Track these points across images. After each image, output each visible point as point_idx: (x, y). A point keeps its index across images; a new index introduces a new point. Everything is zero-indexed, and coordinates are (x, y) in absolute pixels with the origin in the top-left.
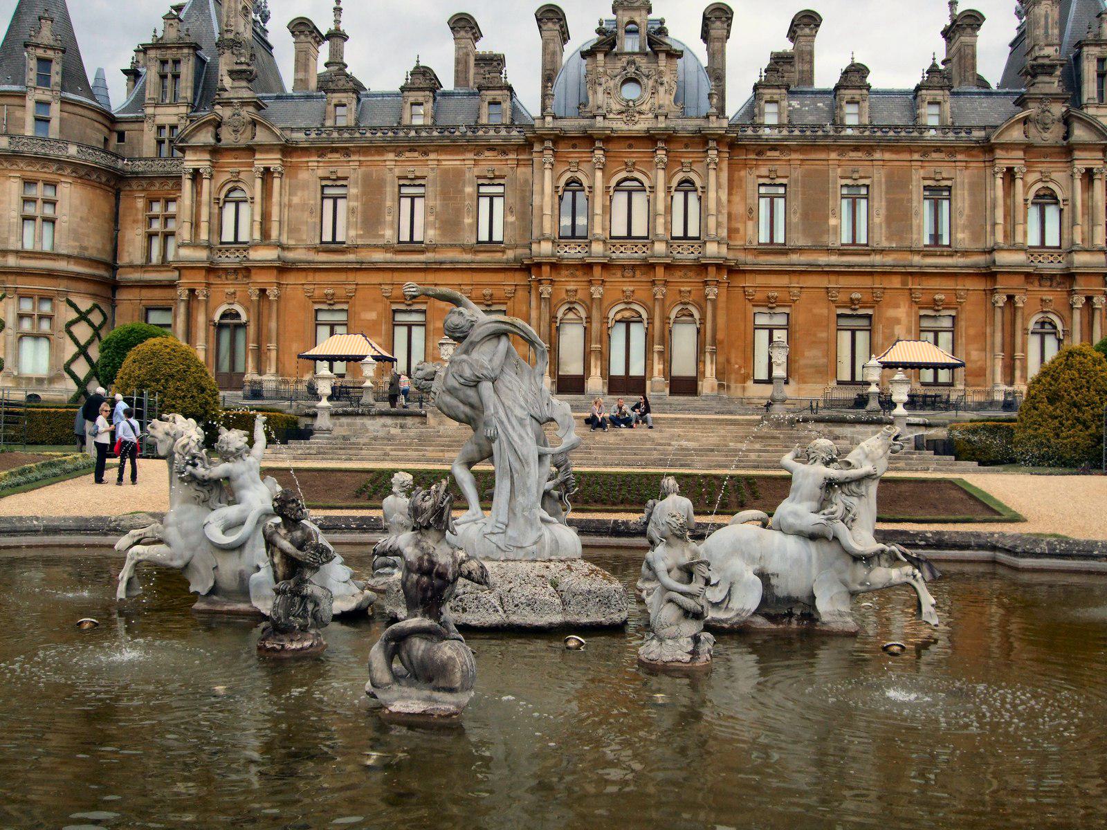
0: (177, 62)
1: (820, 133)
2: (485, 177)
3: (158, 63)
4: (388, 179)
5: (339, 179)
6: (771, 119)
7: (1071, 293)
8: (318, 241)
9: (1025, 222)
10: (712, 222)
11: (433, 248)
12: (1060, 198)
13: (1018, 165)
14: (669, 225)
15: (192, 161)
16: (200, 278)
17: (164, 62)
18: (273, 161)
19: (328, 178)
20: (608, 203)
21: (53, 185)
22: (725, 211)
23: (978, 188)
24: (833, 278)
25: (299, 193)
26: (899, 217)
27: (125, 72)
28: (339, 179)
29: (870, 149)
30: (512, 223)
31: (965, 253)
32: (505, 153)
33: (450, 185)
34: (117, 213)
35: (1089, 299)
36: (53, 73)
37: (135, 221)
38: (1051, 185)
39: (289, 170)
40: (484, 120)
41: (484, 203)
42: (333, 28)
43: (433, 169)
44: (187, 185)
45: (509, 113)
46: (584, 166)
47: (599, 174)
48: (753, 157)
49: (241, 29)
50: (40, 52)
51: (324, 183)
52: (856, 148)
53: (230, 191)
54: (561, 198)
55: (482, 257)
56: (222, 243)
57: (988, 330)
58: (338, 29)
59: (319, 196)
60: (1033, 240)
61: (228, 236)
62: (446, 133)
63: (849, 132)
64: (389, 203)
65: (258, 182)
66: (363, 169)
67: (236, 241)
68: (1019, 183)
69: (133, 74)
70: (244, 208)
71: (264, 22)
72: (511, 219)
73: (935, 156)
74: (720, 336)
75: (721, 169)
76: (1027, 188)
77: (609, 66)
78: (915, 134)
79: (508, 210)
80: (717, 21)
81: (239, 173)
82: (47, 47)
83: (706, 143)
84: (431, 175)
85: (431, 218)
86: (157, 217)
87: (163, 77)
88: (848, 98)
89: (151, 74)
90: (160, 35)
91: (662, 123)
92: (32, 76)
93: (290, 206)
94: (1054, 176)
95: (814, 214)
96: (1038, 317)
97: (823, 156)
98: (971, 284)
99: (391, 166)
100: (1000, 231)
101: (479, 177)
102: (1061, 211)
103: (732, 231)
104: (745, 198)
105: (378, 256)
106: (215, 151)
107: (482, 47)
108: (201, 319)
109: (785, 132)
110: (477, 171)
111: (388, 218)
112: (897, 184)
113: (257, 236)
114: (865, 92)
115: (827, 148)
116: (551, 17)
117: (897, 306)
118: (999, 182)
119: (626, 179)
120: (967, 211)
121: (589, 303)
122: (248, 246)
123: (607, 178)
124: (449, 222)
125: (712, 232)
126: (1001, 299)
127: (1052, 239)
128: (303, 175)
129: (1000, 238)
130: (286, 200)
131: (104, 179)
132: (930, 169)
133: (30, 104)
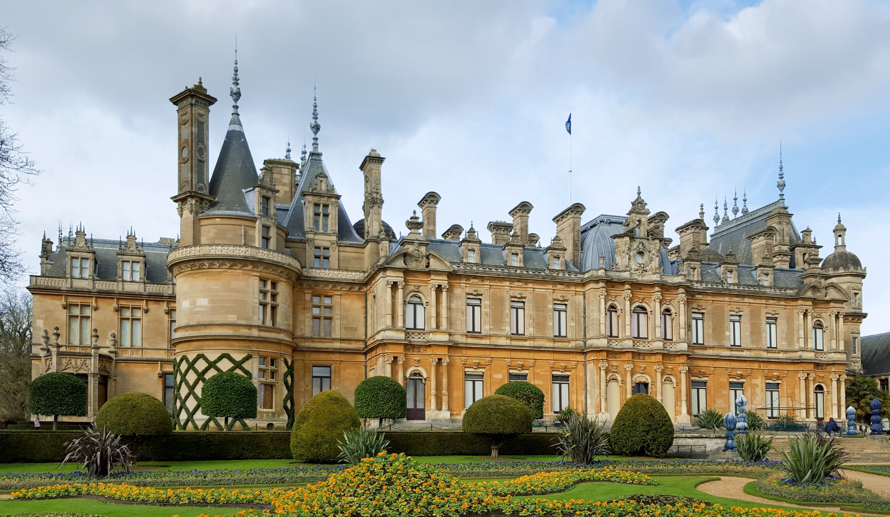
0: (326, 206)
5: (478, 295)
11: (533, 338)
16: (445, 351)
17: (317, 205)
18: (443, 281)
19: (472, 294)
23: (790, 320)
24: (729, 363)
26: (756, 332)
28: (478, 295)
29: (744, 296)
52: (737, 296)
55: (557, 345)
65: (434, 293)
85: (531, 321)
87: (317, 214)
95: (718, 330)
97: (721, 299)
99: (507, 290)
100: (802, 341)
105: (503, 342)
106: (406, 272)
112: (755, 315)
115: (724, 295)
124: (540, 324)
132: (771, 309)
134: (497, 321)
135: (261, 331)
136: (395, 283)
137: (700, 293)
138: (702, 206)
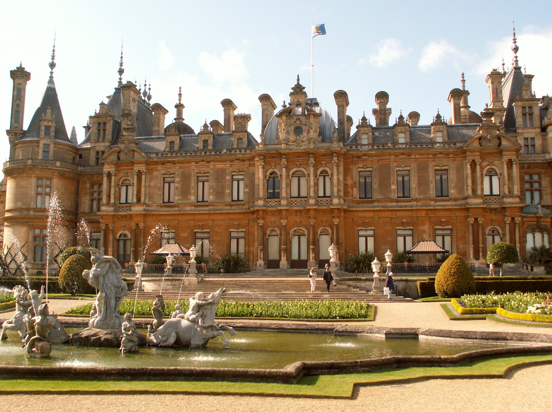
0: (105, 124)
1: (386, 147)
2: (235, 172)
3: (97, 124)
4: (192, 174)
6: (365, 142)
7: (505, 216)
8: (162, 202)
9: (482, 184)
10: (335, 189)
12: (498, 172)
13: (478, 159)
14: (316, 191)
15: (107, 169)
17: (99, 124)
19: (166, 174)
20: (289, 182)
21: (51, 179)
22: (342, 184)
23: (460, 169)
24: (394, 213)
25: (154, 181)
27: (84, 127)
30: (247, 192)
31: (455, 200)
32: (244, 161)
33: (220, 175)
34: (78, 190)
35: (513, 219)
36: (51, 131)
37: (86, 194)
38: (494, 167)
39: (149, 171)
40: (235, 146)
41: (235, 183)
42: (178, 103)
43: (212, 169)
44: (105, 179)
45: (246, 143)
46: (278, 166)
47: (284, 170)
48: (356, 159)
49: (132, 108)
50: (46, 123)
51: (164, 176)
53: (124, 181)
54: (268, 181)
56: (120, 204)
57: (467, 234)
58: (180, 103)
59: (162, 182)
60: (487, 192)
61: (123, 200)
62: (218, 153)
63: (400, 146)
64: (193, 185)
65: (136, 177)
66: (181, 169)
67: (126, 203)
68: (478, 167)
69: (87, 128)
70: (130, 188)
71: (149, 100)
72: (247, 190)
73: (439, 155)
74: (340, 241)
75: (339, 165)
76: (482, 169)
77: (288, 121)
78: (430, 146)
79: (246, 186)
80: (341, 97)
81: (127, 173)
82: (49, 121)
83: (333, 154)
84: (211, 171)
85: (211, 191)
86: (95, 192)
87: (99, 130)
88: (399, 130)
89: (94, 130)
90: (98, 112)
91: (312, 146)
92: (42, 133)
93: (150, 187)
94: (495, 163)
96: (490, 227)
97: (388, 157)
98: (458, 214)
101: (232, 172)
102: (499, 178)
103: (346, 193)
104: (352, 178)
107: (236, 112)
108: (111, 237)
109: (370, 147)
110: (231, 169)
111: (193, 191)
113: (135, 200)
114: (407, 127)
116: (265, 99)
117: (424, 225)
118: (469, 167)
119: (297, 171)
120: (455, 180)
121: (281, 227)
122: (132, 204)
123: (288, 170)
125: (336, 194)
126: (471, 220)
127: (496, 191)
128: (155, 173)
129: (470, 192)
130: (148, 184)
131: (72, 176)
133: (41, 145)
134: (185, 192)
135: (36, 211)
136: (109, 172)
137: (364, 155)
138: (463, 75)
